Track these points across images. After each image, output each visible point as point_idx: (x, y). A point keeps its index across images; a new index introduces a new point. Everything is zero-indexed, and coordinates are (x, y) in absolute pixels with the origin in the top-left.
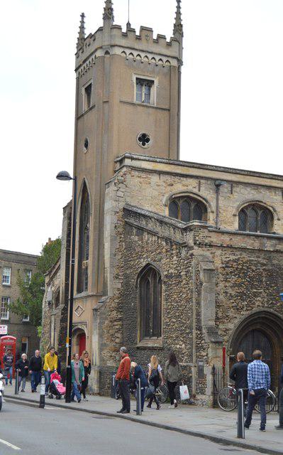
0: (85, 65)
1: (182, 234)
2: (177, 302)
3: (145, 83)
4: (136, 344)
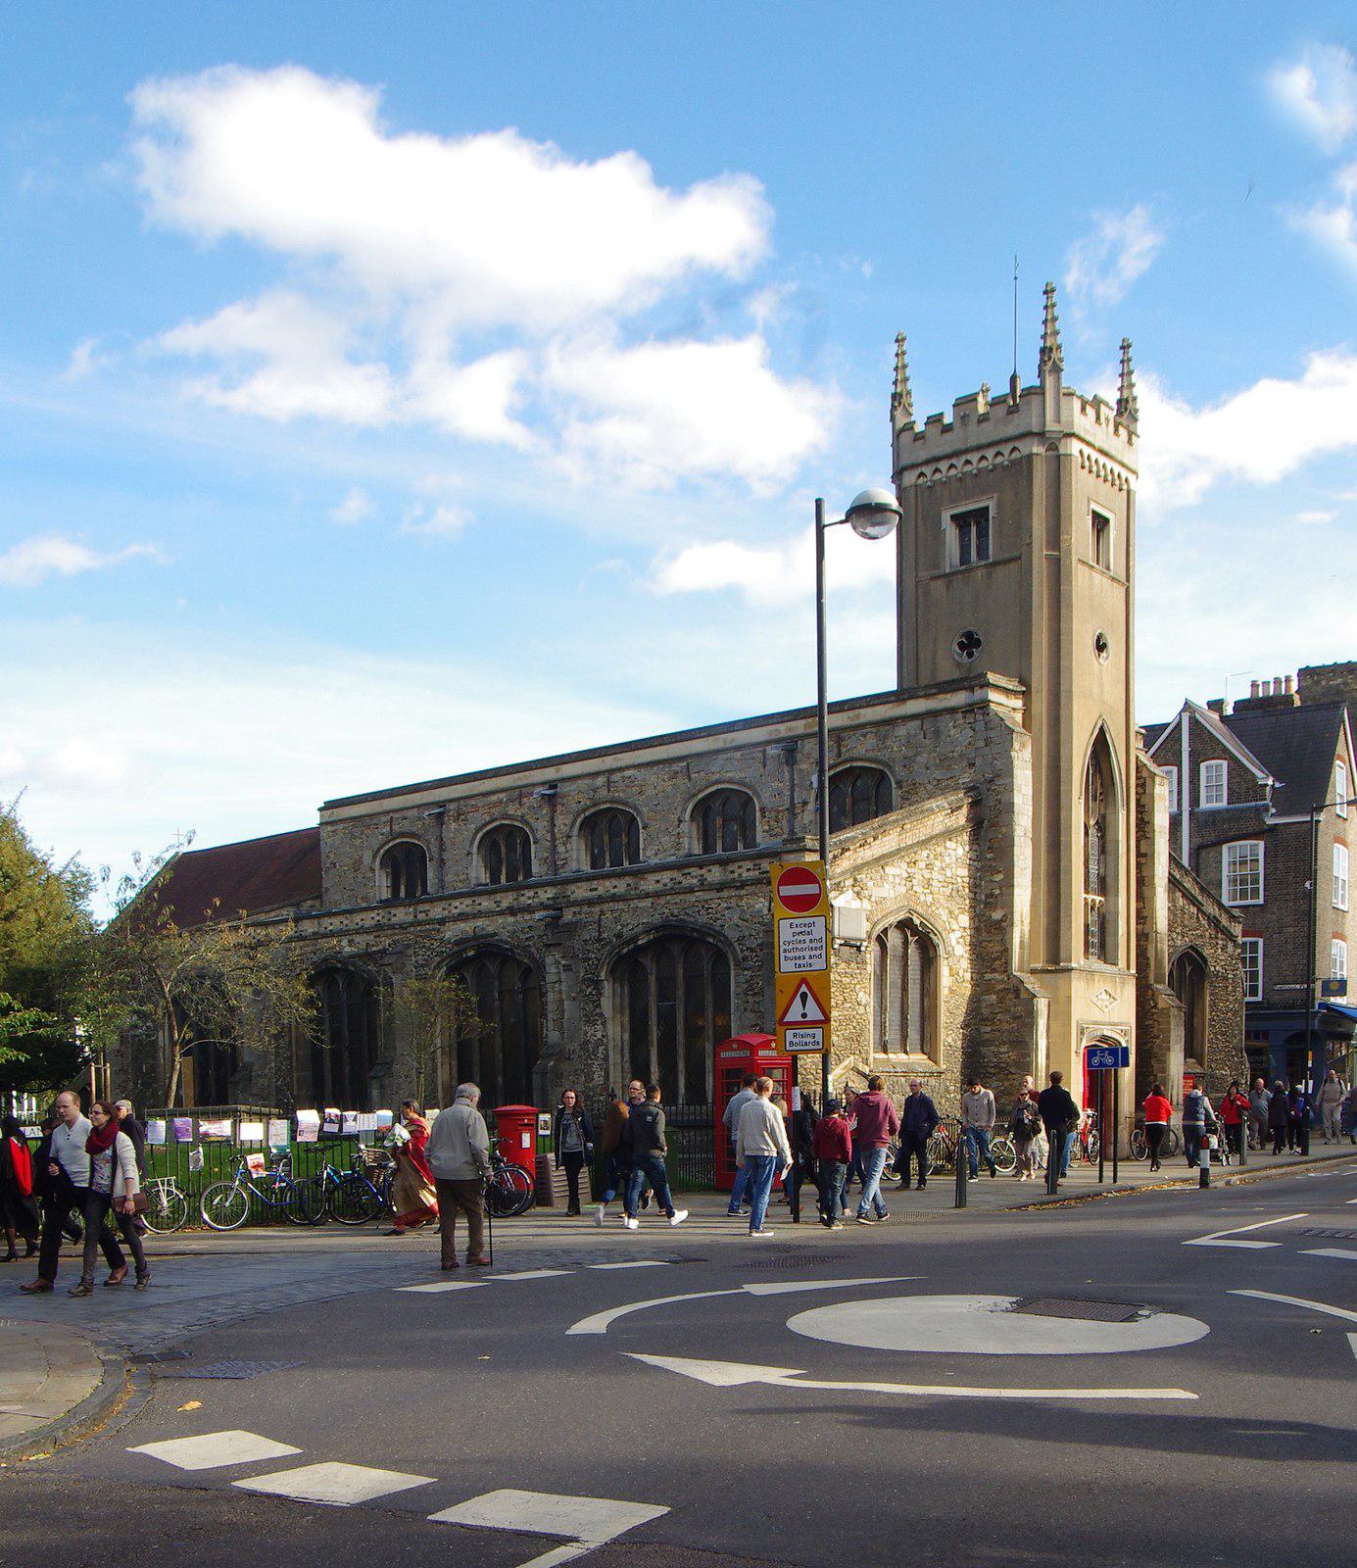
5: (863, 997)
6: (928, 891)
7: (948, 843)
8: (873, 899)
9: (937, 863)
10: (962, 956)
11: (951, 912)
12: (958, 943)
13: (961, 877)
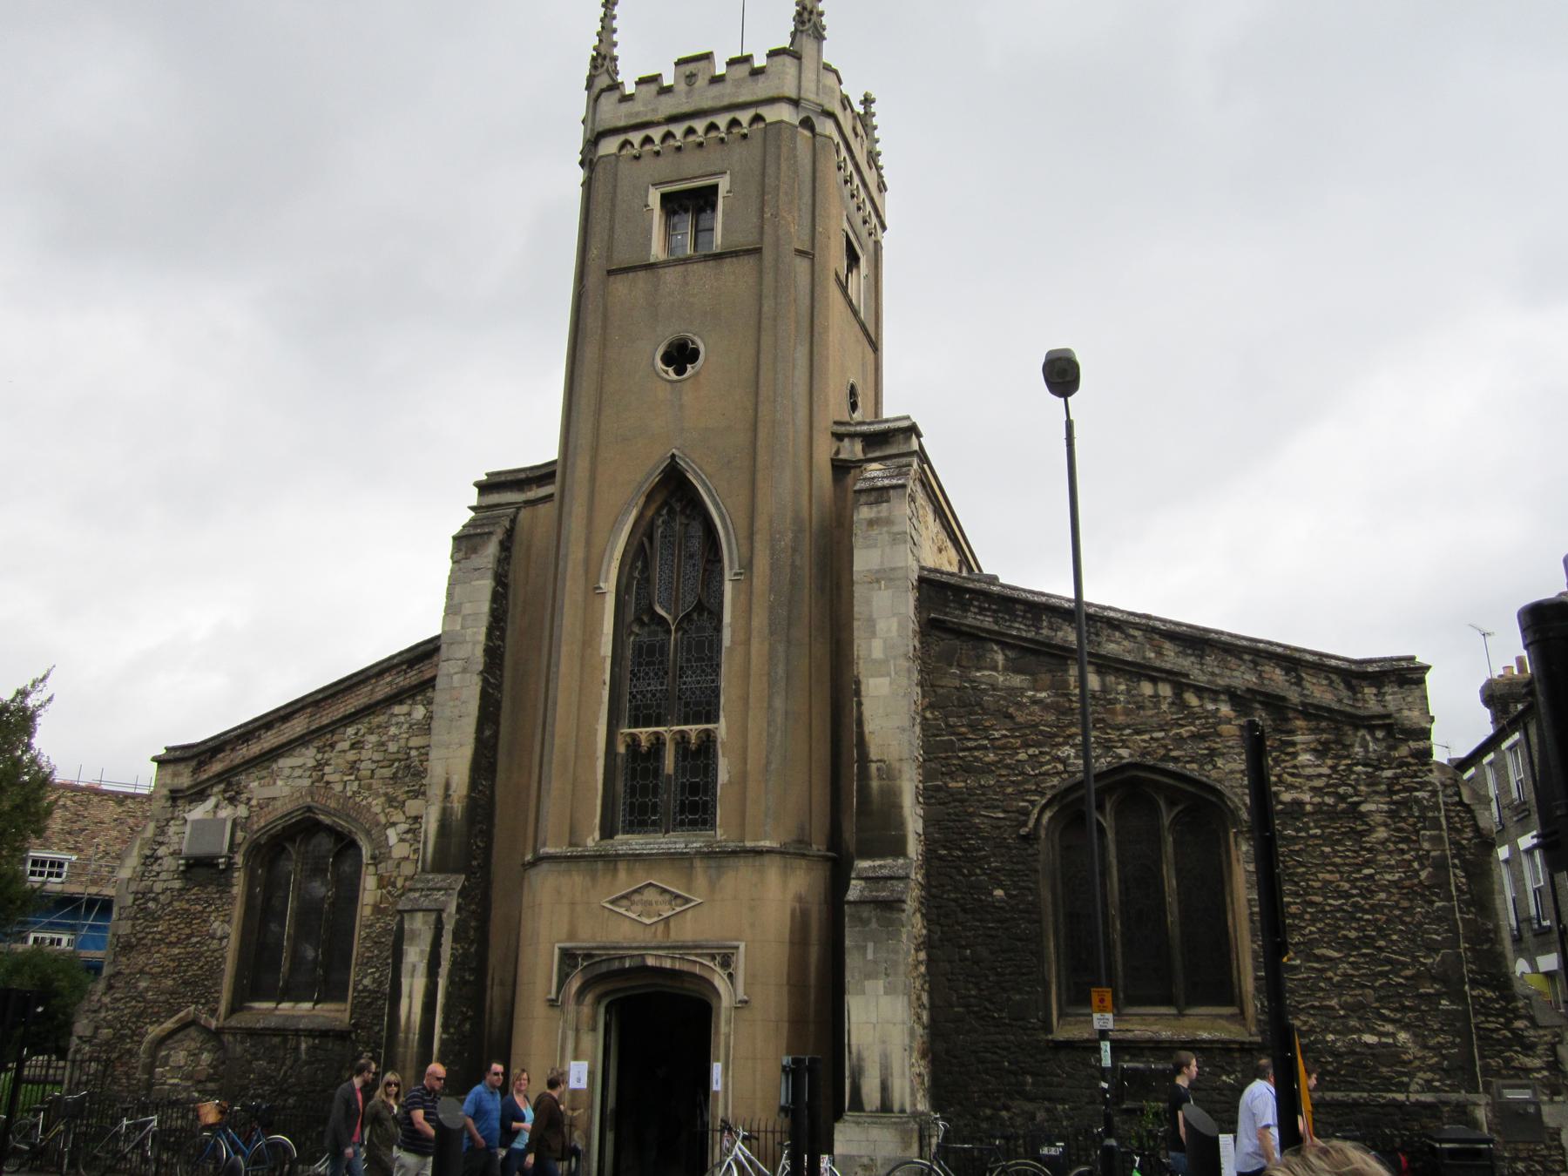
0: (678, 130)
1: (1350, 687)
2: (1347, 895)
3: (853, 259)
4: (1049, 1030)
5: (217, 926)
6: (353, 777)
7: (397, 709)
8: (254, 802)
9: (373, 738)
10: (407, 858)
11: (391, 800)
12: (402, 840)
13: (417, 749)
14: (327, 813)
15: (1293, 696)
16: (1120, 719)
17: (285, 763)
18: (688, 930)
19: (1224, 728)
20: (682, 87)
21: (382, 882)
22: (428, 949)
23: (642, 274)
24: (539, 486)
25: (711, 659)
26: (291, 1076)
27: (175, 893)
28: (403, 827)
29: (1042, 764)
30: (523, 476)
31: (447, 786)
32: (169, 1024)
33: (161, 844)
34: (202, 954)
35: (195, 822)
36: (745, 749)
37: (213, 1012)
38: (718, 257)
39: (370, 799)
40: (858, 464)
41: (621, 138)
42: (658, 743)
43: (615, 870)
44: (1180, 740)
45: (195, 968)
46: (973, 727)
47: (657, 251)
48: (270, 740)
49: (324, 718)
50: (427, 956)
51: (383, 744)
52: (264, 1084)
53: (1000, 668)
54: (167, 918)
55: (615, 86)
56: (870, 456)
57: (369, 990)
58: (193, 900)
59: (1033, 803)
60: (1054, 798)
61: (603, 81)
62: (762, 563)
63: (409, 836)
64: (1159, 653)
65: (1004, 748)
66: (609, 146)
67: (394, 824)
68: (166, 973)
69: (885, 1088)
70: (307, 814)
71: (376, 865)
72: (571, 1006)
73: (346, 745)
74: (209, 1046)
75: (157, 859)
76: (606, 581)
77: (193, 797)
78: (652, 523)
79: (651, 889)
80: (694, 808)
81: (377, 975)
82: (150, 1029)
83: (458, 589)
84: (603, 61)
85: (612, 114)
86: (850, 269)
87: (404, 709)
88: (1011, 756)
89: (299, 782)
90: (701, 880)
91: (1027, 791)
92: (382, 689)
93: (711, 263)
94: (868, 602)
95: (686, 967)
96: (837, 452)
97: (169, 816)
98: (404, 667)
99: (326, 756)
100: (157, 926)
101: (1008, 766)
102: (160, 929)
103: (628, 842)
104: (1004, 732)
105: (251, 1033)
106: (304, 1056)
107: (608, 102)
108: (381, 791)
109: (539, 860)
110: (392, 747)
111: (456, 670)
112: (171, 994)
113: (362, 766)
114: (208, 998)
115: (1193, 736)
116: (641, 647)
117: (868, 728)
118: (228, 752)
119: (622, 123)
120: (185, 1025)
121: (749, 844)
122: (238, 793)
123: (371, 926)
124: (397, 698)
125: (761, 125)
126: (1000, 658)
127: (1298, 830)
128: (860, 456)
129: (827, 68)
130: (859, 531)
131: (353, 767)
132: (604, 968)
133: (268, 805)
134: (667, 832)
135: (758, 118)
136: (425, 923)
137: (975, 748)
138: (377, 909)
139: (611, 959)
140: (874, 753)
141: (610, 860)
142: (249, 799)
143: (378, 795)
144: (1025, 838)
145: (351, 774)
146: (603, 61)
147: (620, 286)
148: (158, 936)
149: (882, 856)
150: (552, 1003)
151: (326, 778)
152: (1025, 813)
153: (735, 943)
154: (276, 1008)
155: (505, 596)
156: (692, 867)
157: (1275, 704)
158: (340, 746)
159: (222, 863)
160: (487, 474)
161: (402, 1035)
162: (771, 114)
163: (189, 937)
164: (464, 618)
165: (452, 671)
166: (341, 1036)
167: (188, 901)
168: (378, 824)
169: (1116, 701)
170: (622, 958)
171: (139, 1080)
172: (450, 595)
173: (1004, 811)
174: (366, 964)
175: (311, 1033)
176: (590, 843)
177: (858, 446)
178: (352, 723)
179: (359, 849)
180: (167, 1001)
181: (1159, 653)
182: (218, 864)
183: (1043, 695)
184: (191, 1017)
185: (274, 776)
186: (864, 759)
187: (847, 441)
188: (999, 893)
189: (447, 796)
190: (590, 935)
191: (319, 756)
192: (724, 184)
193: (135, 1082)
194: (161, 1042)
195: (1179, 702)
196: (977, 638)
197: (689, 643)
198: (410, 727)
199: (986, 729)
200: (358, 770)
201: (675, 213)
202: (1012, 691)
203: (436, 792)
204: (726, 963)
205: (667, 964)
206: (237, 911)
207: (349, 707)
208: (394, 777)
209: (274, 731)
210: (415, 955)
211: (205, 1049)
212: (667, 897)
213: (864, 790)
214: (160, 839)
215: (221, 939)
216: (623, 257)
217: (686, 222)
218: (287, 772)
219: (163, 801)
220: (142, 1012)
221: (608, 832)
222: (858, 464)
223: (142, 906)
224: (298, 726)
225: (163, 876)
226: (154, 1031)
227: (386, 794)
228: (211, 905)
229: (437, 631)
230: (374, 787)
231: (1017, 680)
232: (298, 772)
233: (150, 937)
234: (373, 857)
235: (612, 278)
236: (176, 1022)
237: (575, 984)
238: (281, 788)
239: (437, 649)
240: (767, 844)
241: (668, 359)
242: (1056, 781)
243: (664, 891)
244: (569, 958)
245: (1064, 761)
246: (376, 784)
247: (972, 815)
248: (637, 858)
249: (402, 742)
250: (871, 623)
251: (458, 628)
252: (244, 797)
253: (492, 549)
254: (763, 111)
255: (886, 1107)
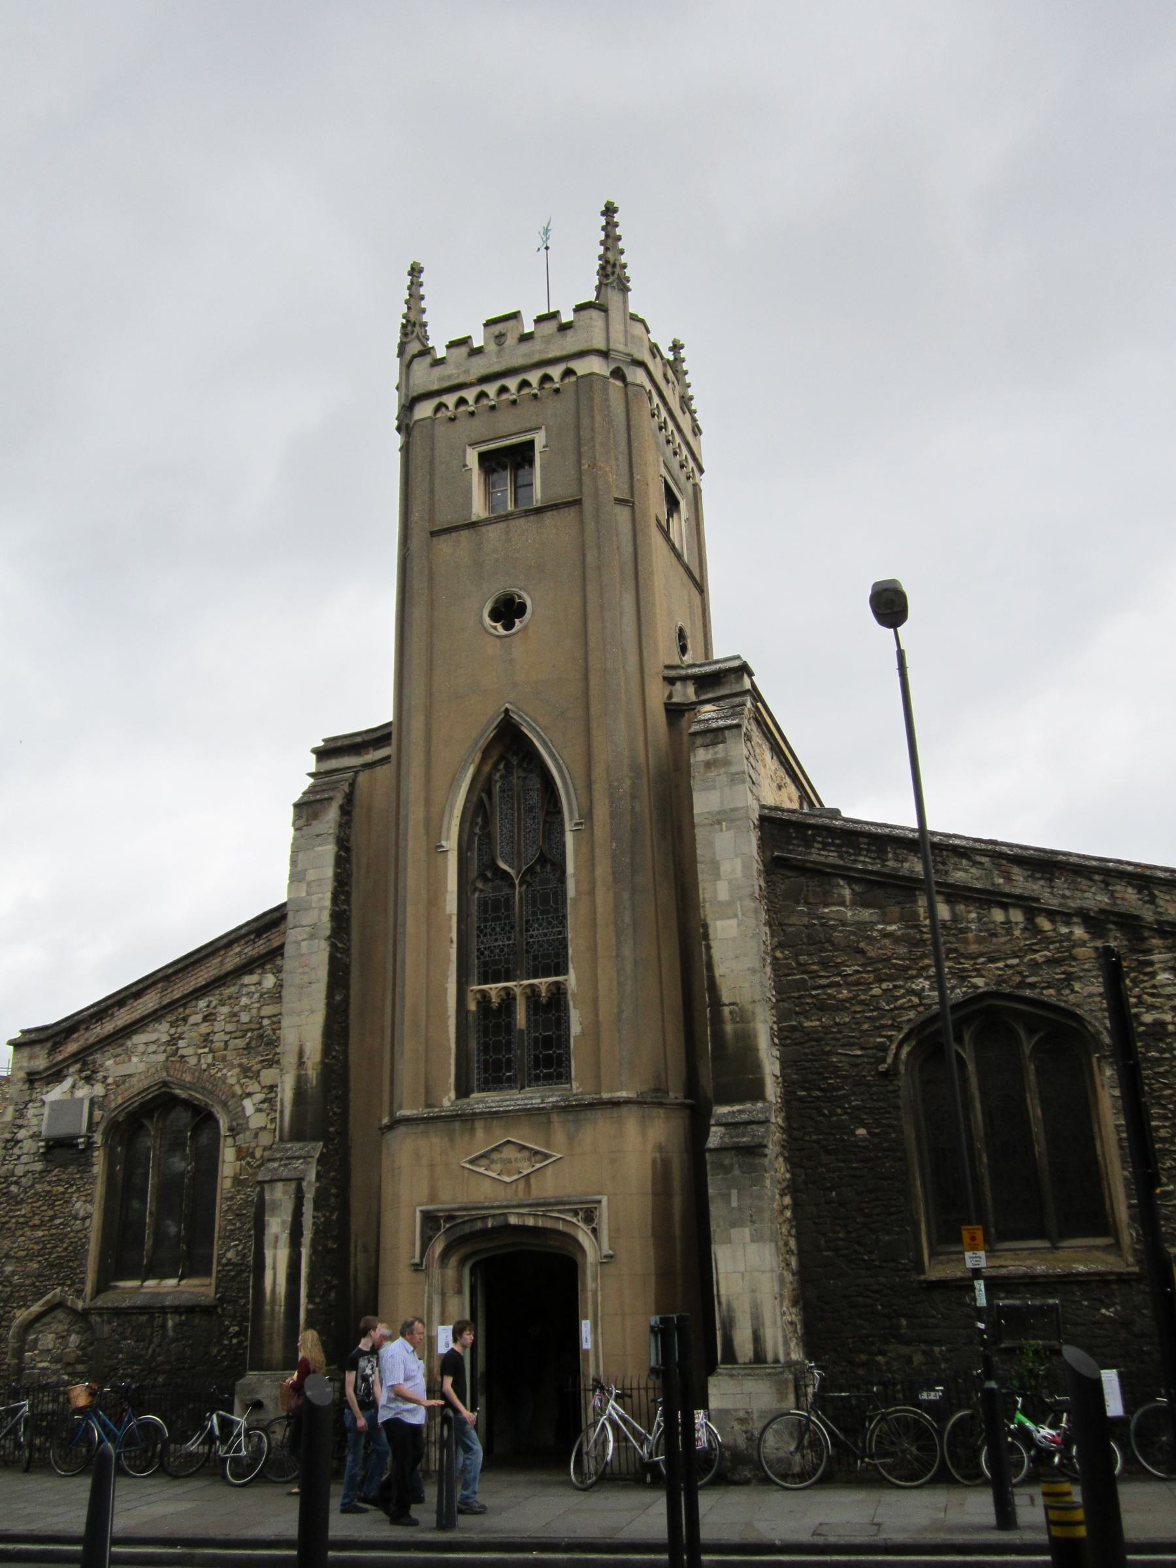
0: (491, 389)
3: (673, 503)
4: (919, 1267)
5: (79, 1207)
6: (206, 1050)
7: (247, 979)
8: (110, 1080)
9: (225, 1010)
10: (263, 1128)
11: (245, 1071)
12: (259, 1110)
13: (269, 1017)
14: (182, 1087)
15: (1148, 915)
16: (974, 948)
17: (139, 1039)
18: (549, 1186)
19: (1080, 951)
20: (492, 347)
21: (241, 1154)
22: (290, 1219)
23: (464, 534)
24: (376, 749)
25: (556, 910)
26: (159, 1355)
27: (37, 1175)
28: (259, 1097)
29: (897, 998)
30: (359, 739)
31: (301, 1054)
32: (36, 1308)
33: (20, 1127)
34: (66, 1235)
35: (52, 1103)
36: (595, 1001)
37: (79, 1293)
38: (539, 511)
39: (225, 1071)
40: (692, 707)
41: (435, 402)
42: (508, 998)
43: (472, 1130)
44: (1035, 965)
45: (60, 1250)
46: (824, 964)
47: (478, 509)
48: (123, 1017)
49: (175, 992)
50: (288, 1225)
51: (235, 1015)
52: (133, 1363)
53: (848, 903)
54: (30, 1201)
55: (426, 351)
56: (703, 697)
57: (232, 1264)
58: (54, 1181)
59: (890, 1038)
60: (911, 1031)
61: (414, 347)
62: (601, 811)
63: (265, 1106)
64: (1008, 879)
65: (857, 983)
66: (424, 410)
67: (249, 1095)
68: (31, 1257)
69: (757, 1339)
70: (163, 1090)
71: (234, 1137)
72: (436, 1270)
73: (197, 1018)
74: (76, 1328)
75: (18, 1142)
76: (448, 839)
77: (50, 1079)
78: (489, 779)
79: (511, 1147)
80: (548, 1061)
81: (240, 1248)
82: (18, 1313)
83: (301, 855)
84: (413, 328)
85: (424, 377)
86: (670, 514)
87: (254, 978)
88: (865, 991)
89: (154, 1058)
90: (559, 1136)
91: (883, 1027)
92: (231, 960)
93: (531, 518)
94: (711, 844)
95: (549, 1224)
96: (670, 696)
97: (27, 1098)
98: (252, 937)
99: (179, 1030)
100: (20, 1210)
101: (862, 1002)
102: (23, 1212)
103: (484, 1100)
104: (856, 968)
105: (117, 1312)
106: (171, 1333)
107: (421, 367)
108: (236, 1062)
109: (396, 1123)
110: (245, 1017)
111: (304, 936)
112: (40, 1276)
113: (216, 1038)
114: (74, 1282)
115: (1050, 962)
116: (486, 904)
117: (718, 972)
118: (83, 1032)
119: (435, 387)
120: (52, 1308)
121: (605, 1096)
122: (94, 1072)
123: (231, 1198)
124: (247, 968)
125: (573, 379)
126: (847, 893)
127: (1162, 1051)
128: (693, 698)
129: (634, 318)
130: (697, 775)
131: (207, 1039)
132: (467, 1229)
133: (124, 1082)
134: (523, 1088)
135: (569, 372)
136: (285, 1192)
137: (830, 986)
138: (237, 1181)
139: (474, 1220)
140: (726, 997)
141: (467, 1119)
142: (105, 1078)
143: (233, 1067)
144: (885, 1075)
145: (205, 1047)
146: (413, 328)
147: (444, 545)
148: (22, 1220)
149: (741, 1100)
150: (416, 1268)
151: (180, 1052)
152: (884, 1048)
153: (598, 1197)
154: (141, 1286)
155: (348, 860)
156: (549, 1122)
157: (1129, 924)
158: (193, 1019)
159: (81, 1143)
160: (324, 740)
161: (268, 1308)
162: (582, 367)
163: (52, 1218)
164: (309, 884)
165: (300, 938)
166: (207, 1311)
167: (49, 1183)
168: (234, 1095)
169: (968, 930)
170: (484, 1218)
171: (9, 1365)
172: (294, 862)
173: (862, 1048)
174: (229, 1237)
175: (176, 1310)
176: (446, 1103)
177: (691, 690)
178: (204, 995)
179: (217, 1122)
180: (33, 1284)
181: (1008, 879)
182: (77, 1145)
183: (894, 927)
184: (57, 1299)
185: (129, 1053)
186: (716, 1003)
187: (678, 685)
188: (861, 1132)
189: (301, 1064)
190: (451, 1197)
191: (173, 1031)
192: (540, 439)
193: (5, 1367)
194: (29, 1325)
195: (1031, 928)
196: (822, 874)
197: (534, 896)
198: (261, 996)
199: (838, 965)
200: (212, 1041)
201: (493, 471)
202: (862, 926)
203: (289, 1060)
204: (589, 1218)
205: (530, 1222)
206: (99, 1190)
207: (200, 979)
208: (248, 1047)
209: (126, 1009)
210: (277, 1226)
211: (74, 1331)
212: (526, 1154)
213: (718, 1035)
214: (19, 1122)
215: (84, 1219)
216: (446, 517)
217: (505, 480)
218: (141, 1048)
219: (21, 1084)
220: (10, 1295)
221: (463, 1090)
222: (692, 707)
223: (5, 1191)
224: (150, 1002)
225: (24, 1159)
226: (22, 1315)
227: (240, 1065)
228: (71, 1185)
229: (284, 899)
230: (228, 1058)
231: (866, 914)
232: (153, 1048)
233: (13, 1220)
234: (231, 1129)
235: (435, 540)
236: (43, 1305)
237: (438, 1247)
238: (136, 1065)
239: (284, 917)
240: (623, 1094)
241: (496, 615)
242: (912, 1014)
243: (523, 1148)
244: (430, 1219)
245: (918, 994)
246: (230, 1055)
247: (829, 1053)
248: (492, 1116)
249: (254, 1012)
250: (715, 865)
251: (304, 894)
252: (100, 1075)
253: (332, 814)
254: (575, 365)
255: (759, 1357)
